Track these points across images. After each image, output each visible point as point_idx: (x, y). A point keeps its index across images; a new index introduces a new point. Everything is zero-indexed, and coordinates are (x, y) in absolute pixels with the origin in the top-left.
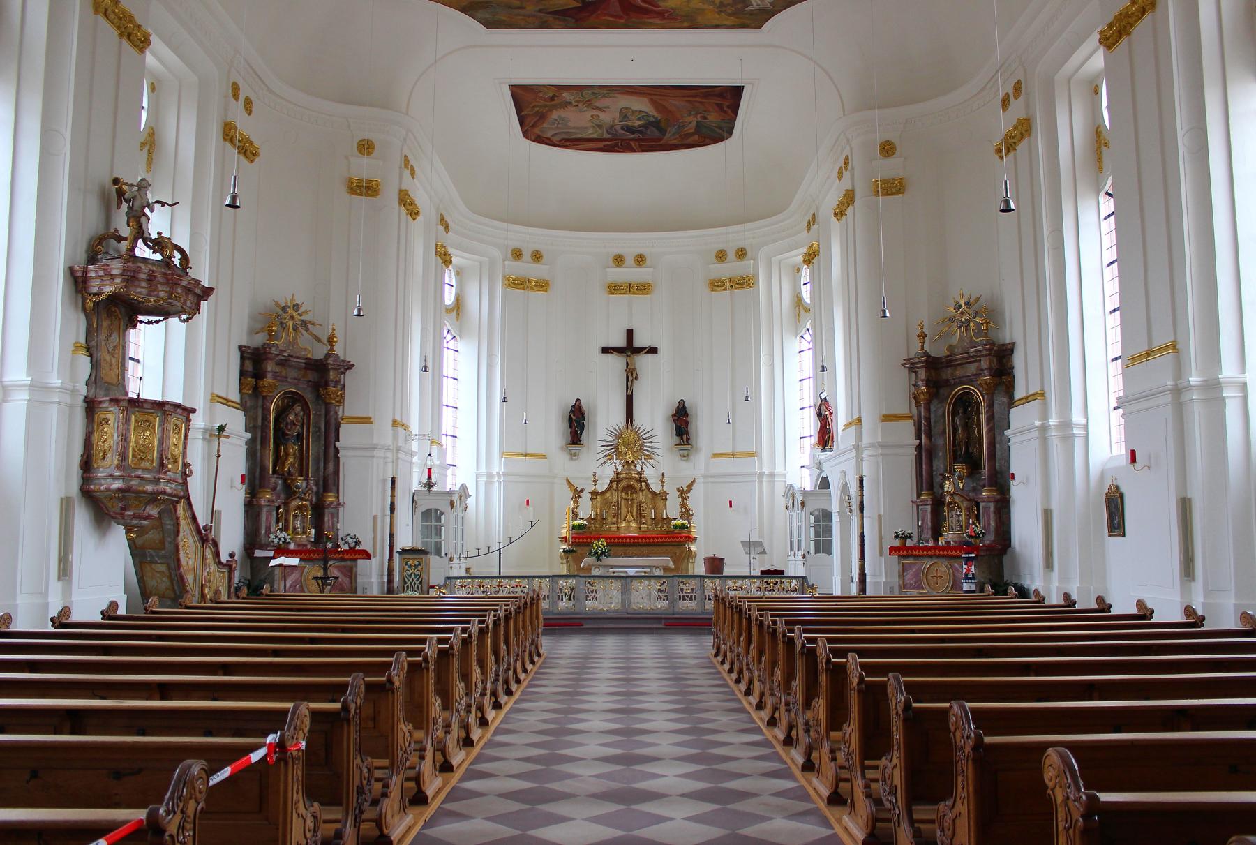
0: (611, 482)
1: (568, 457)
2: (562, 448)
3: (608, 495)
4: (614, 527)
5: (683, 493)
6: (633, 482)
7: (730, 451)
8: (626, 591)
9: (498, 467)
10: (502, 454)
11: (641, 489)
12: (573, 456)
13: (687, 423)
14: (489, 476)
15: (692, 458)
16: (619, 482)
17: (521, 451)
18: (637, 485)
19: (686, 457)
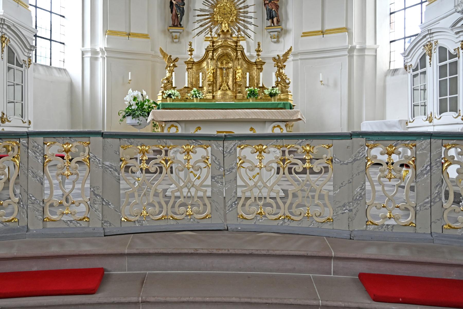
0: (207, 51)
1: (169, 40)
2: (164, 32)
3: (204, 64)
4: (209, 96)
5: (280, 62)
6: (229, 50)
7: (320, 29)
8: (224, 172)
9: (101, 43)
10: (105, 32)
11: (237, 58)
12: (174, 39)
13: (277, 7)
14: (94, 52)
15: (281, 39)
16: (214, 50)
17: (123, 29)
18: (233, 54)
19: (277, 39)
